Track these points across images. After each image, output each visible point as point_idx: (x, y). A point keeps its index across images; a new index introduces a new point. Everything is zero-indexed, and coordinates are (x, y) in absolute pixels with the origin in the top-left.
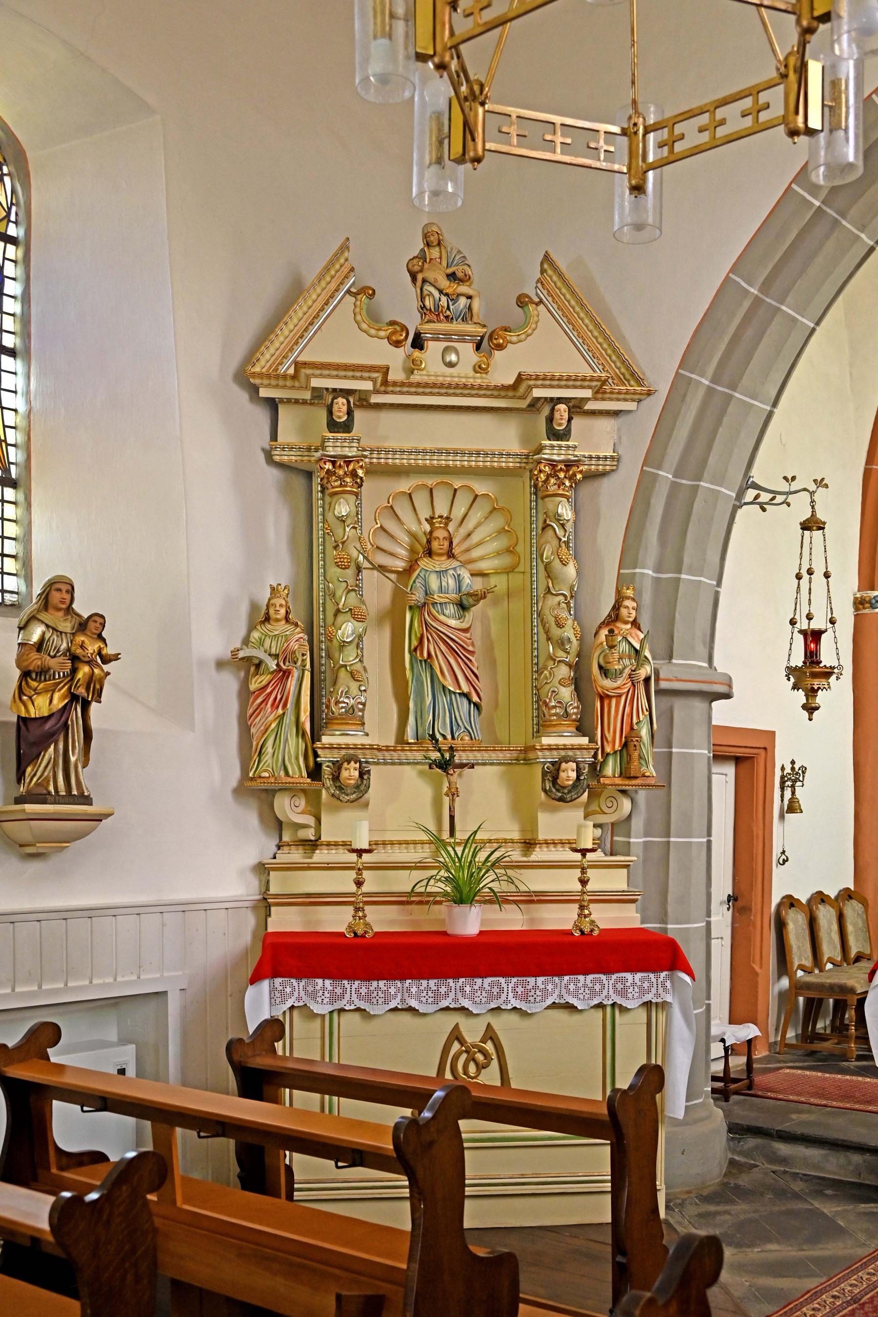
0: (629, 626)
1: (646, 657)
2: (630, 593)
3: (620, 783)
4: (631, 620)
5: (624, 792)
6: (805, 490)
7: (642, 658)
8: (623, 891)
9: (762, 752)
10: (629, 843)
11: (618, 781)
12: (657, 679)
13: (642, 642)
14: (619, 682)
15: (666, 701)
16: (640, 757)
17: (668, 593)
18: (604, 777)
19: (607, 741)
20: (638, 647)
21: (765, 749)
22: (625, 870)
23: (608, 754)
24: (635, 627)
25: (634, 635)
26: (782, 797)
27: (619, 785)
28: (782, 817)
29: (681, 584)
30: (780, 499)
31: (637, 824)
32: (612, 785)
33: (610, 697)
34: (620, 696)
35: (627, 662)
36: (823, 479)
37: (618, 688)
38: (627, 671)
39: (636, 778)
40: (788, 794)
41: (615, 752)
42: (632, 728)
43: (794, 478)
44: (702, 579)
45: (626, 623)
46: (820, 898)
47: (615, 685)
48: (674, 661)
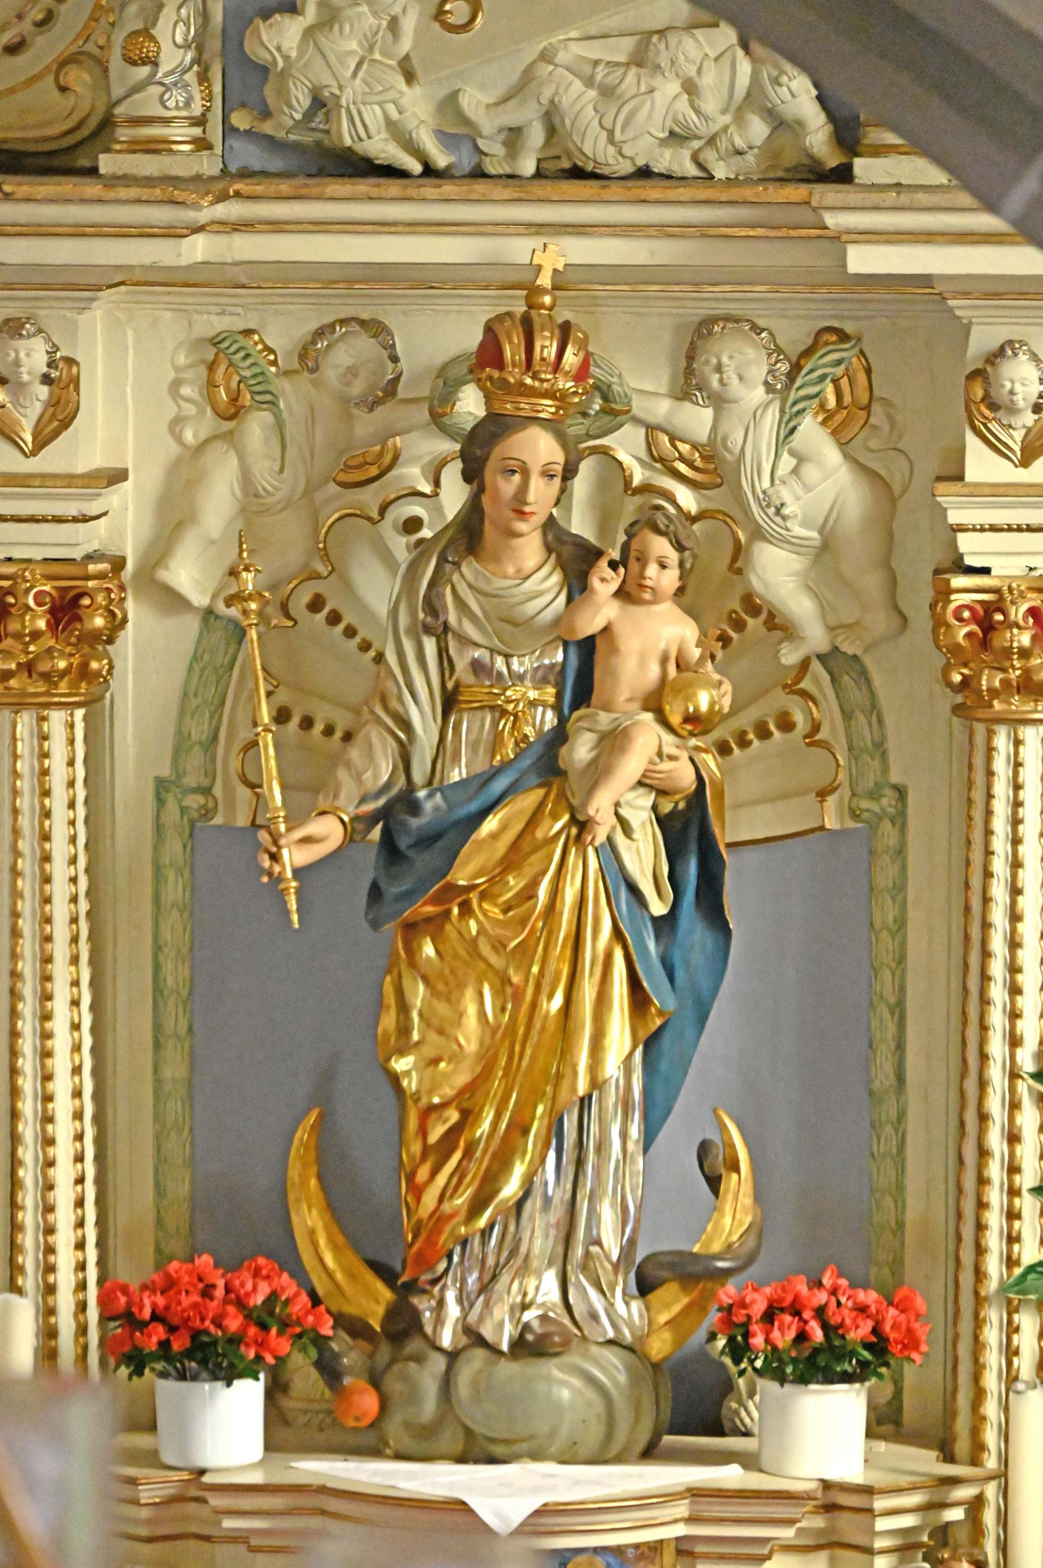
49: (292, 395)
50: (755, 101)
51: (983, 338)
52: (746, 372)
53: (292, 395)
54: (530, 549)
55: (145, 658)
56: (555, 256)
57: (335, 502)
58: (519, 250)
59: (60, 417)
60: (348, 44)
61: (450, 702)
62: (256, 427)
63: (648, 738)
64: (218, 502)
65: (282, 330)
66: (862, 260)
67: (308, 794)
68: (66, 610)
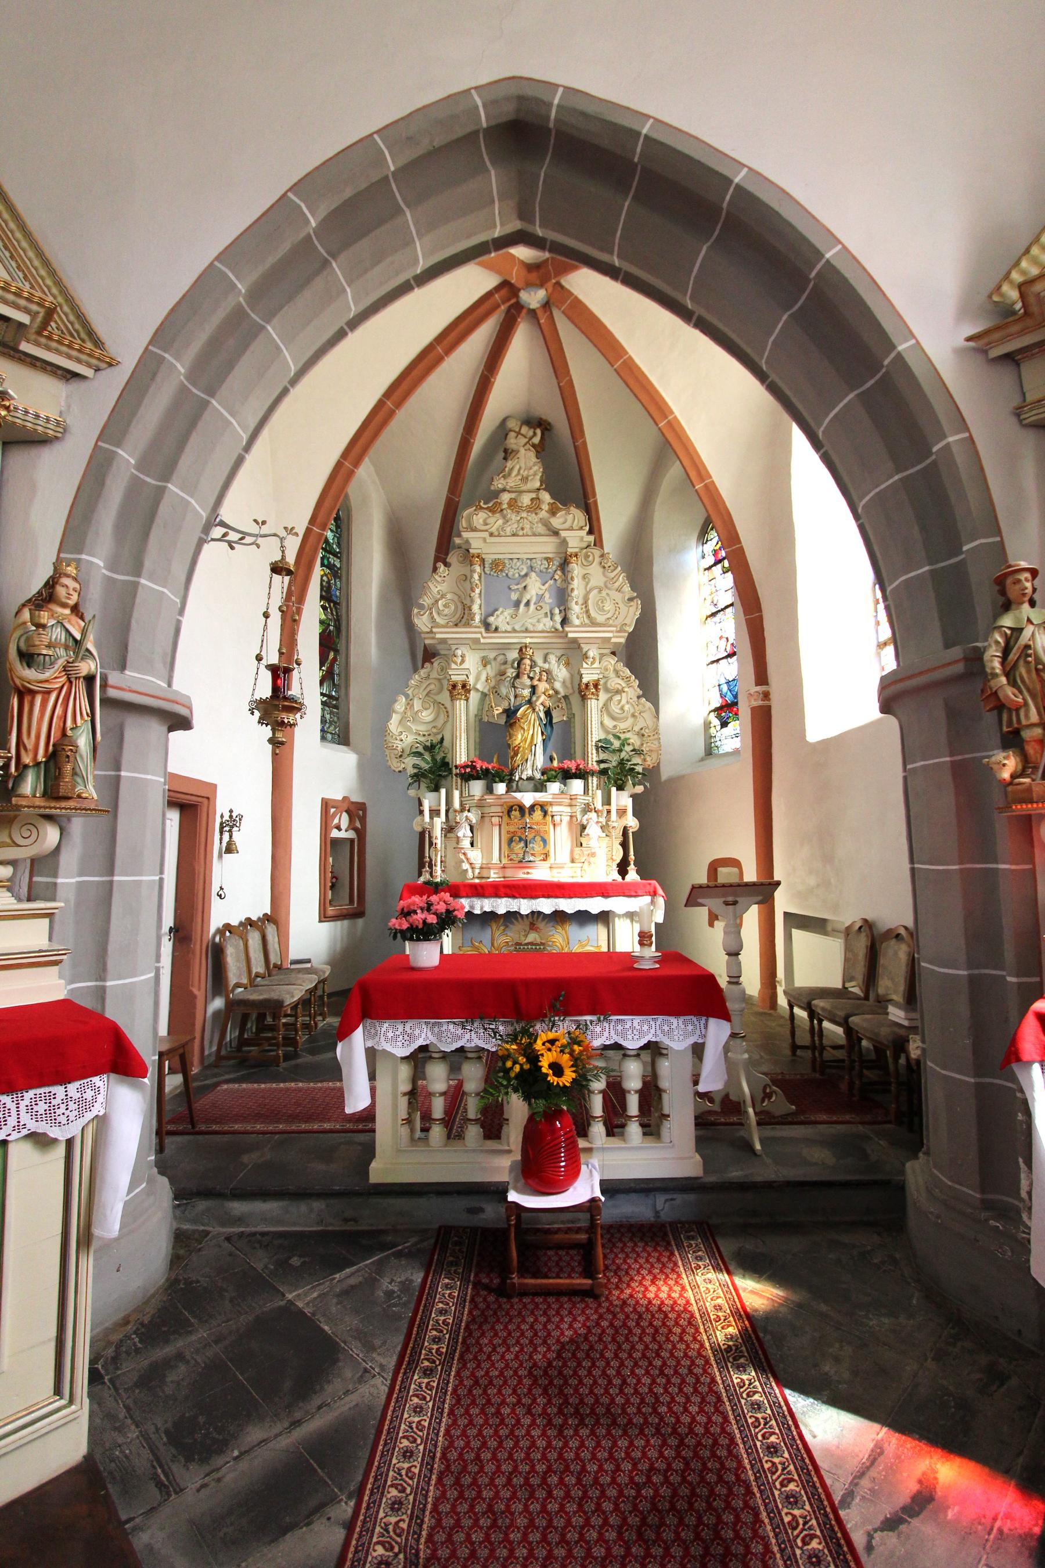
0: (67, 611)
1: (87, 650)
2: (71, 570)
3: (43, 804)
4: (71, 602)
5: (49, 818)
6: (275, 535)
7: (84, 649)
8: (40, 951)
9: (205, 801)
10: (55, 884)
11: (39, 802)
12: (104, 685)
13: (84, 632)
14: (47, 675)
15: (115, 715)
16: (75, 773)
17: (124, 602)
18: (19, 796)
19: (26, 749)
20: (78, 637)
21: (208, 798)
22: (47, 920)
23: (26, 766)
24: (77, 615)
25: (73, 622)
26: (221, 839)
27: (40, 807)
28: (220, 856)
29: (140, 588)
30: (249, 540)
31: (69, 859)
32: (29, 807)
33: (33, 693)
34: (48, 692)
35: (61, 652)
36: (293, 528)
37: (47, 681)
38: (61, 662)
39: (67, 798)
40: (226, 837)
41: (37, 764)
42: (64, 734)
43: (264, 523)
44: (165, 590)
45: (64, 605)
46: (249, 922)
47: (42, 677)
48: (127, 672)
49: (493, 663)
50: (553, 627)
51: (585, 650)
52: (552, 659)
53: (493, 663)
54: (526, 676)
55: (474, 697)
56: (528, 640)
57: (499, 678)
58: (524, 641)
59: (463, 661)
60: (500, 619)
61: (516, 697)
62: (489, 667)
63: (543, 698)
64: (483, 677)
65: (492, 655)
66: (570, 635)
67: (496, 706)
68: (464, 686)
